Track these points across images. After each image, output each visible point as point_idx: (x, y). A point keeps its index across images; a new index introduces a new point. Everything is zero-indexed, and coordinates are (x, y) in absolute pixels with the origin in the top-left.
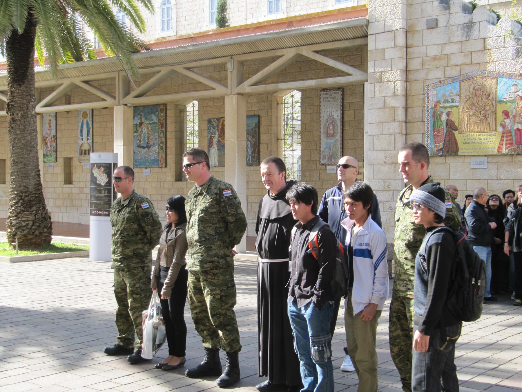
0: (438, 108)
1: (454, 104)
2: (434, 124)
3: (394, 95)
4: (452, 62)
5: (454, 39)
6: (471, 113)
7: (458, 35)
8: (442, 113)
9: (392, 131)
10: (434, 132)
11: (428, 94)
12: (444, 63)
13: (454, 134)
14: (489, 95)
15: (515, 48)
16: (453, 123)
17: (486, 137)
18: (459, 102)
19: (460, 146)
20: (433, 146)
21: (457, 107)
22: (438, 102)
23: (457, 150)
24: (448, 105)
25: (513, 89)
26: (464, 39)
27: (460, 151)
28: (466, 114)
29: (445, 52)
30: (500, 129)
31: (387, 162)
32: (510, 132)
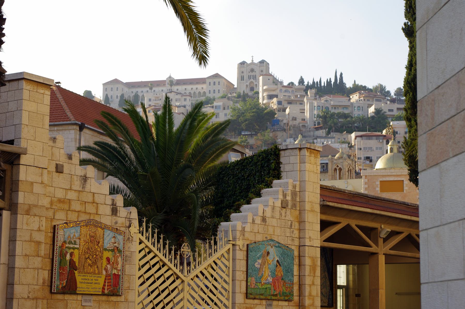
0: (64, 248)
1: (76, 246)
2: (60, 262)
3: (39, 230)
4: (73, 208)
5: (74, 188)
6: (87, 256)
7: (77, 185)
8: (67, 252)
9: (36, 266)
12: (66, 207)
13: (75, 273)
14: (99, 242)
15: (111, 207)
16: (74, 262)
17: (95, 278)
19: (79, 285)
20: (59, 283)
21: (78, 249)
22: (65, 242)
23: (76, 288)
24: (71, 246)
25: (113, 240)
26: (81, 189)
27: (78, 289)
29: (68, 197)
30: (104, 272)
31: (31, 297)
32: (110, 276)
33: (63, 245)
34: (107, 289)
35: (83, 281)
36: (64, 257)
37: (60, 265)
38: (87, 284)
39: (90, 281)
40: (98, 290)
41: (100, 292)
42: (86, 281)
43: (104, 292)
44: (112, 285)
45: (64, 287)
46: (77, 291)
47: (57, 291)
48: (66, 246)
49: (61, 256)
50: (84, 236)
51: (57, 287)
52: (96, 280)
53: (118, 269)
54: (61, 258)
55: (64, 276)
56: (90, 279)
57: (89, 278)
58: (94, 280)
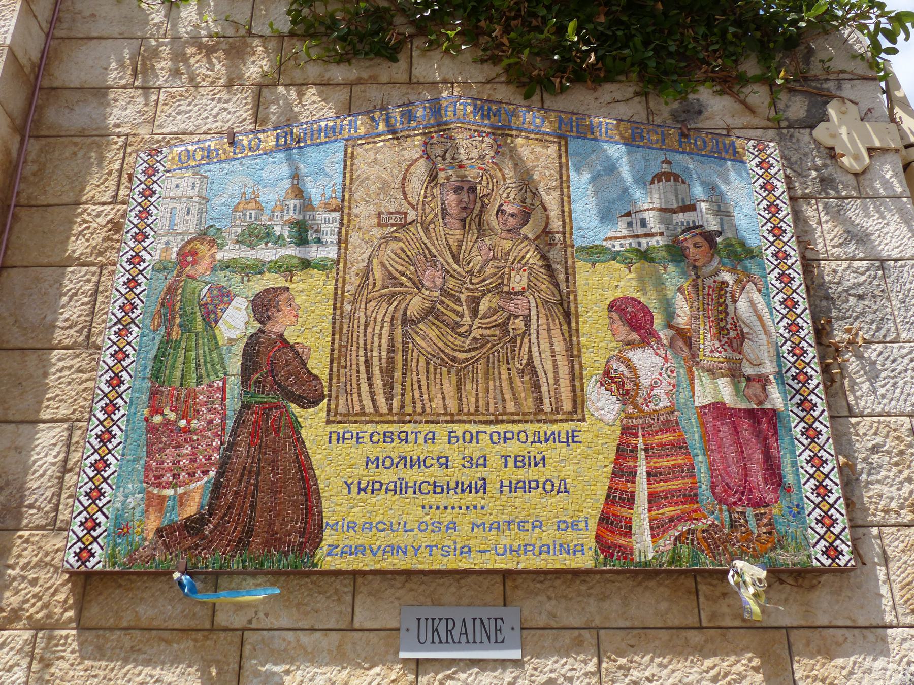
6: (416, 305)
8: (225, 296)
10: (156, 410)
11: (148, 193)
13: (295, 426)
16: (298, 356)
17: (513, 448)
18: (343, 242)
21: (322, 266)
24: (268, 254)
27: (329, 537)
28: (383, 312)
33: (194, 253)
34: (658, 529)
35: (388, 476)
36: (199, 326)
37: (156, 375)
38: (432, 499)
39: (455, 474)
40: (548, 535)
41: (579, 549)
42: (412, 475)
43: (626, 553)
44: (704, 488)
45: (193, 526)
46: (320, 553)
47: (112, 557)
48: (219, 256)
49: (168, 321)
50: (385, 188)
51: (122, 530)
52: (520, 462)
53: (749, 371)
54: (169, 335)
55: (187, 449)
56: (455, 458)
57: (441, 446)
58: (495, 461)
